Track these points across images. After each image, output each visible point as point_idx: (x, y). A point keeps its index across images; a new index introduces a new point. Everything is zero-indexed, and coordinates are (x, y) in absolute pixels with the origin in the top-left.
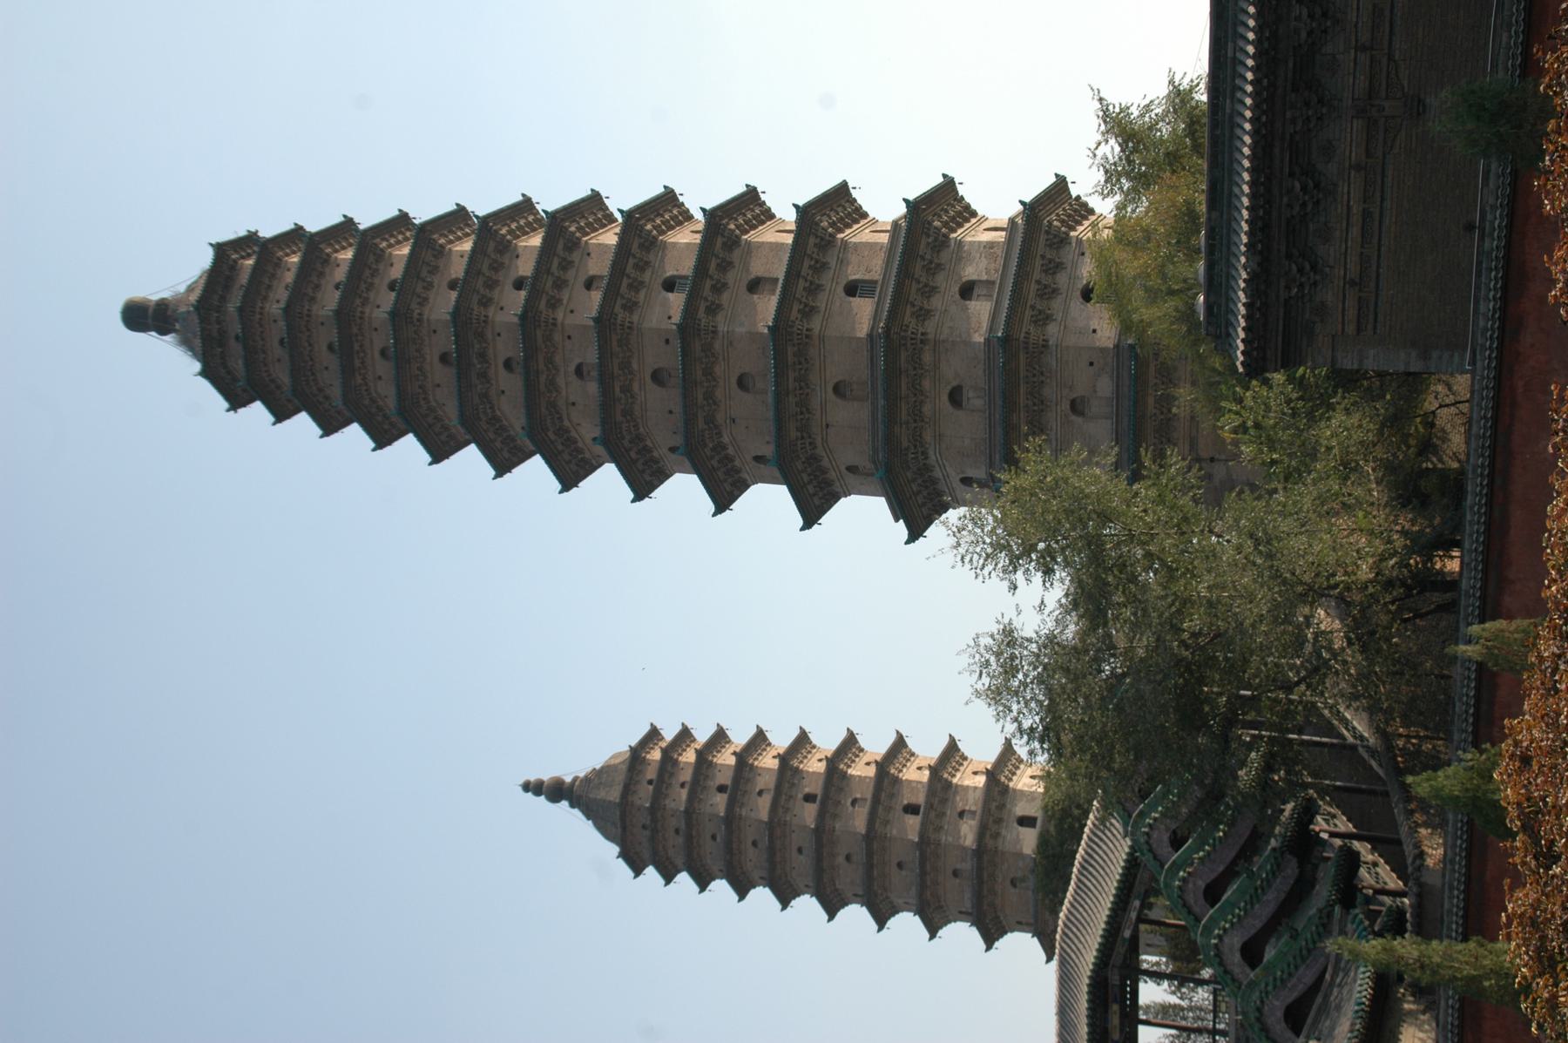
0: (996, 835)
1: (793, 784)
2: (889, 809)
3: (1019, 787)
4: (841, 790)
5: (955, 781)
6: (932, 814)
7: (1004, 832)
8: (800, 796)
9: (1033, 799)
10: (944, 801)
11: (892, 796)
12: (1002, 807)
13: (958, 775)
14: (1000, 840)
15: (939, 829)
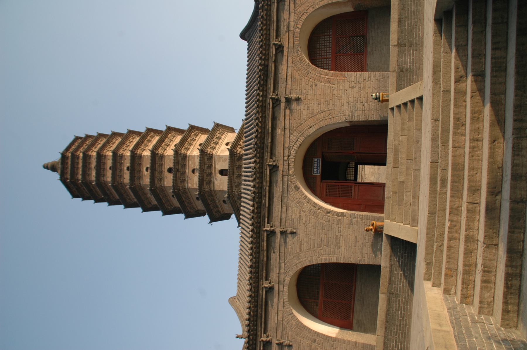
0: (210, 182)
1: (122, 163)
2: (161, 172)
3: (218, 153)
4: (140, 164)
5: (189, 153)
6: (179, 174)
7: (213, 179)
8: (125, 168)
9: (225, 160)
10: (184, 166)
11: (161, 165)
12: (210, 166)
13: (191, 148)
14: (212, 184)
15: (183, 181)
